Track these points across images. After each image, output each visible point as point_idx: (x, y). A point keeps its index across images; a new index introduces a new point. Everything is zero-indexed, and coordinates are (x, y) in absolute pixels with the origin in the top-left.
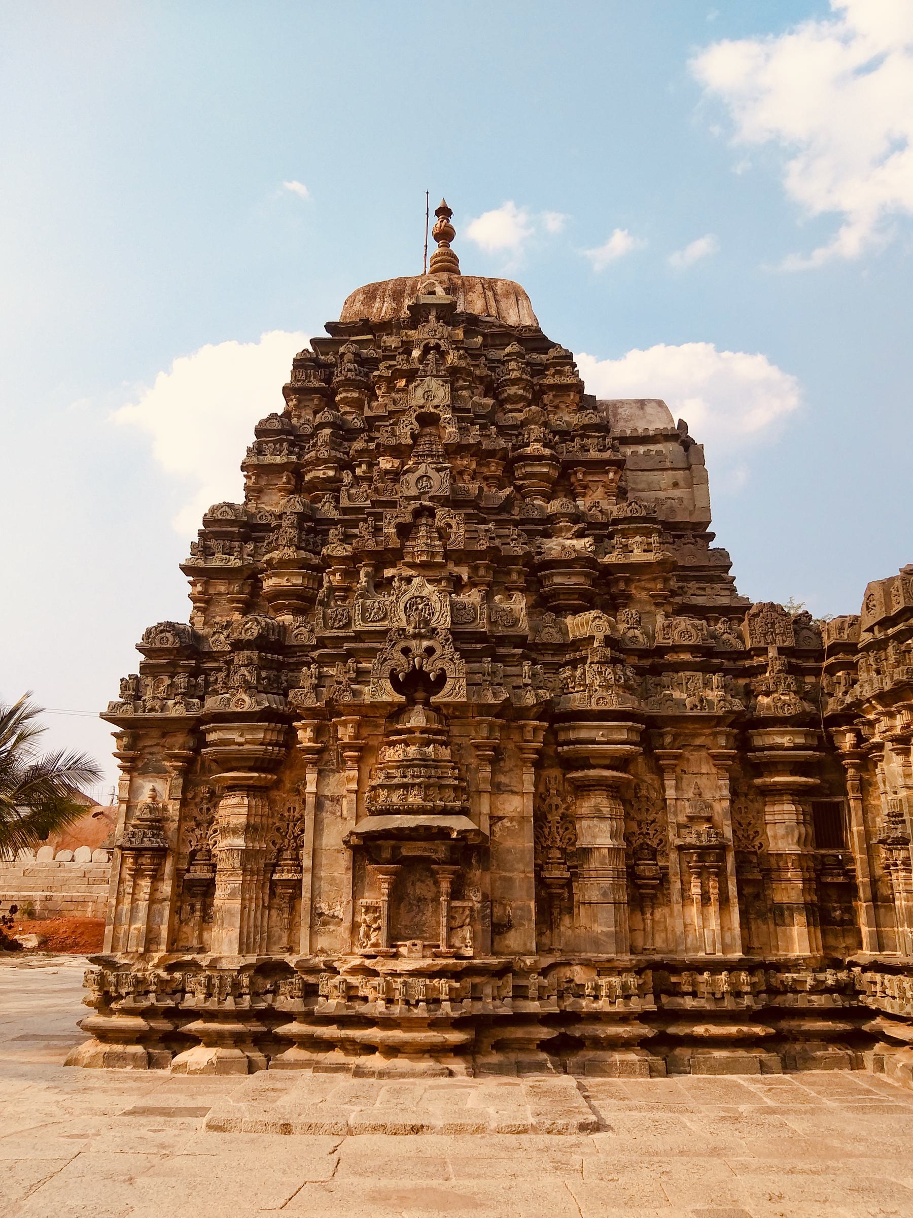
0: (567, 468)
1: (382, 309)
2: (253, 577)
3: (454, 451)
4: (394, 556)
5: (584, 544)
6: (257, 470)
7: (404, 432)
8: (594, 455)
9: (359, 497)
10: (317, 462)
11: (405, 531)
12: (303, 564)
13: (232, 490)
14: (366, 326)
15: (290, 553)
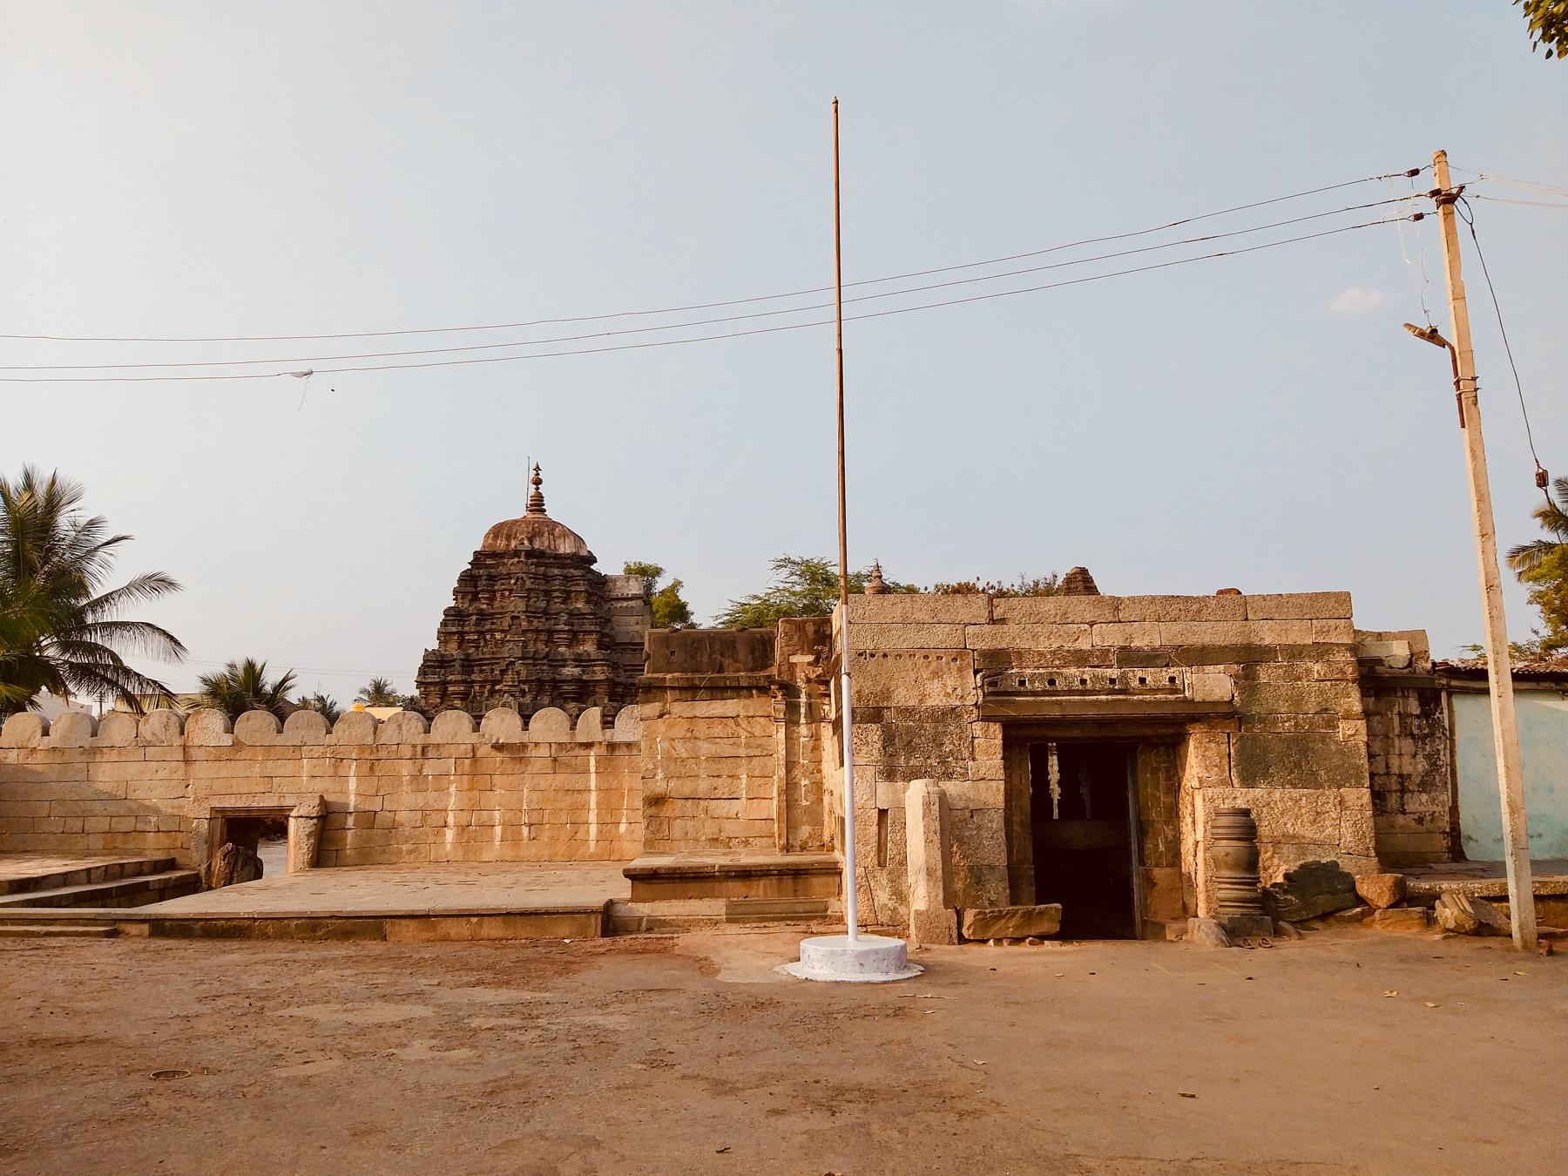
0: (575, 633)
1: (501, 544)
2: (445, 684)
3: (524, 632)
4: (500, 682)
5: (577, 671)
6: (444, 636)
7: (506, 622)
8: (587, 627)
9: (486, 652)
10: (468, 633)
11: (503, 672)
12: (464, 682)
13: (434, 645)
14: (494, 555)
15: (459, 678)
